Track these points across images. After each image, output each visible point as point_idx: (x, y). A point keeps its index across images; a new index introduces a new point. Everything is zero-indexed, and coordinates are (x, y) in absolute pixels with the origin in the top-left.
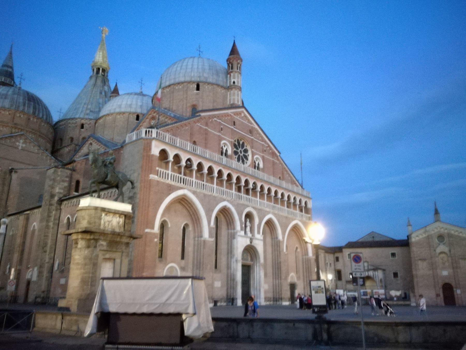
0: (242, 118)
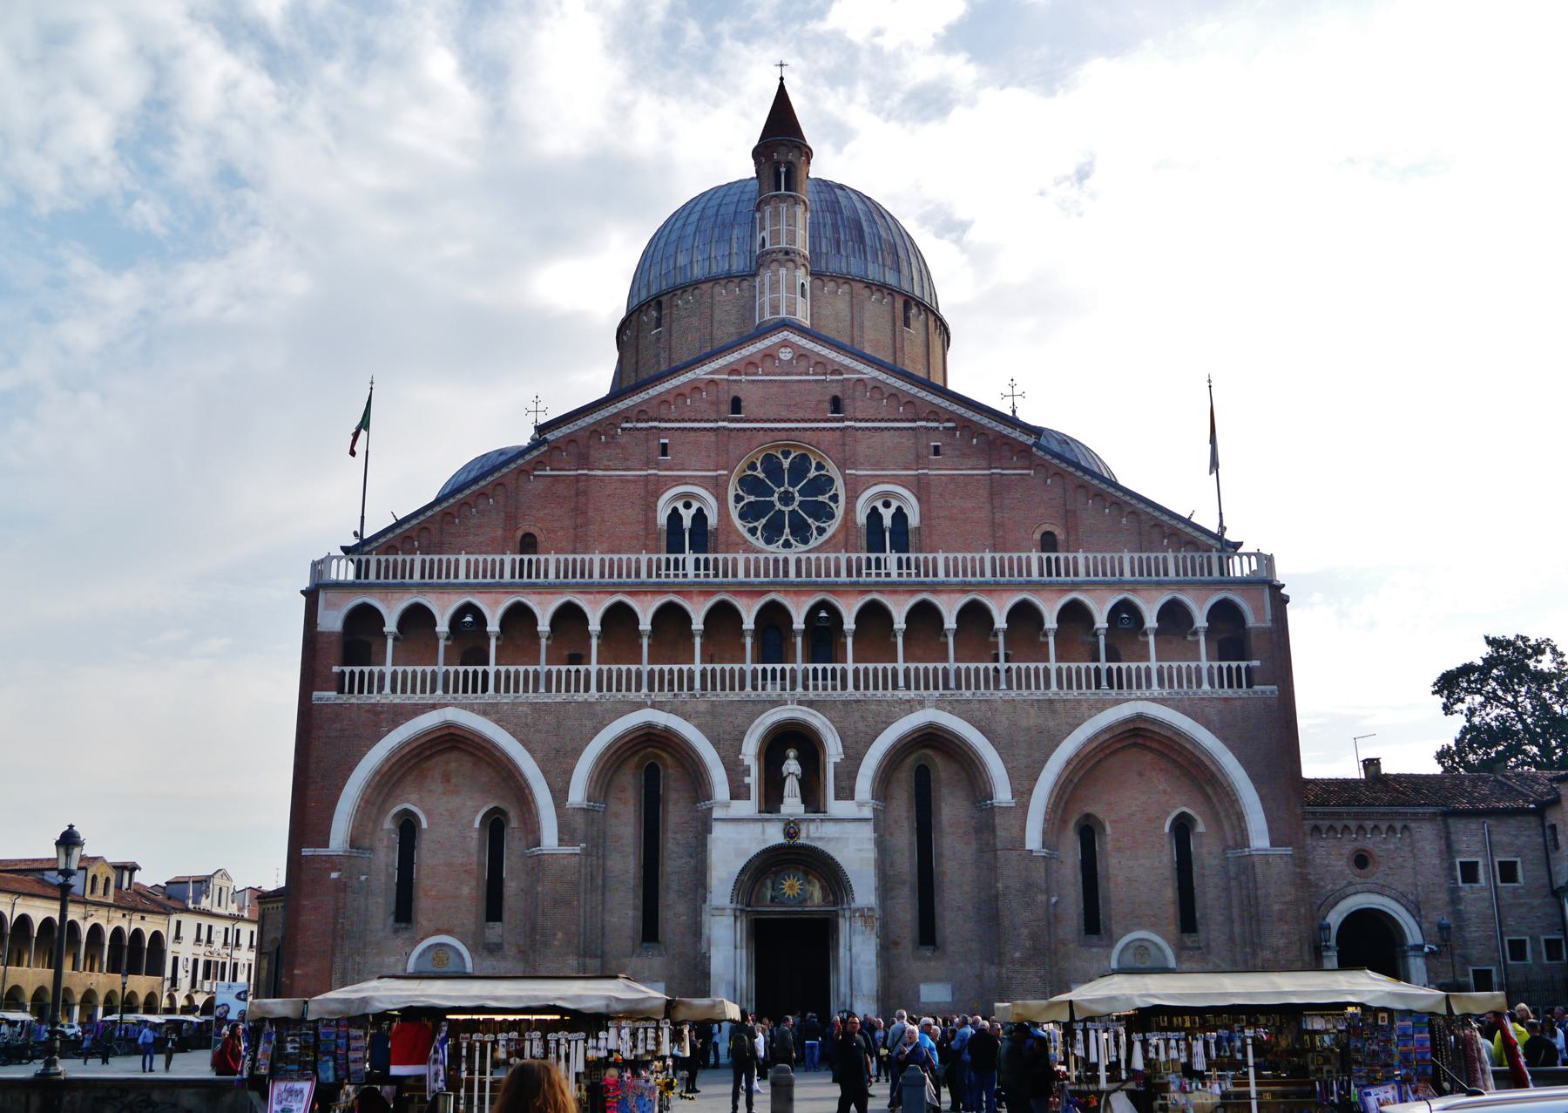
0: (787, 368)
